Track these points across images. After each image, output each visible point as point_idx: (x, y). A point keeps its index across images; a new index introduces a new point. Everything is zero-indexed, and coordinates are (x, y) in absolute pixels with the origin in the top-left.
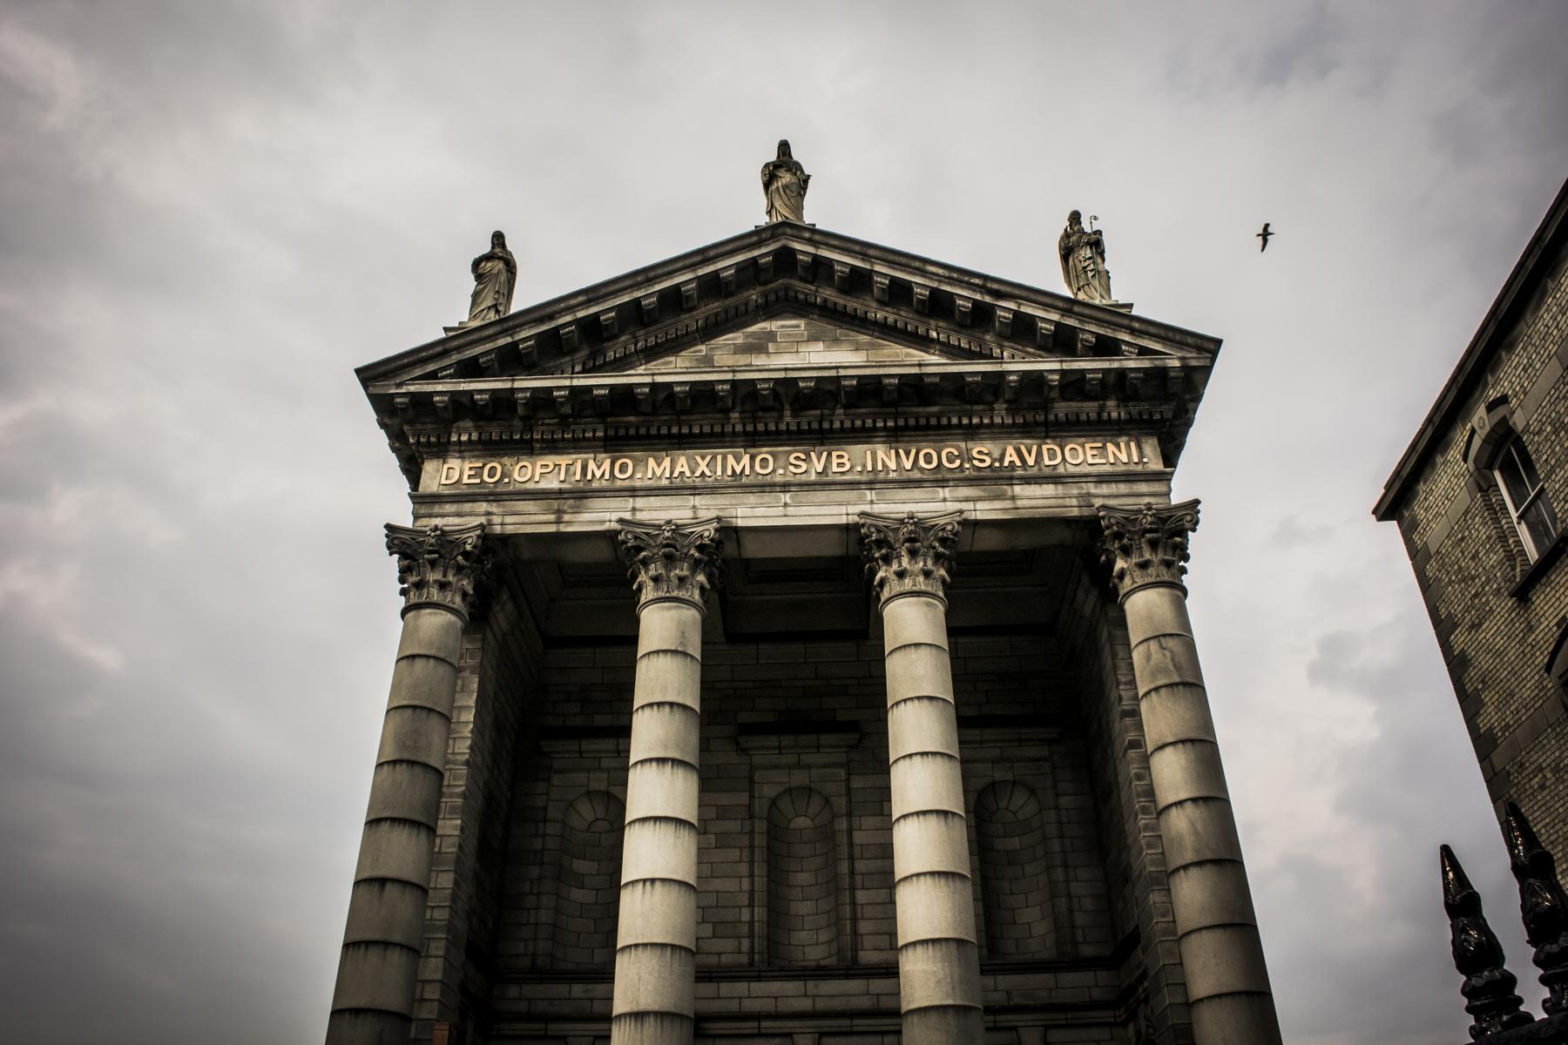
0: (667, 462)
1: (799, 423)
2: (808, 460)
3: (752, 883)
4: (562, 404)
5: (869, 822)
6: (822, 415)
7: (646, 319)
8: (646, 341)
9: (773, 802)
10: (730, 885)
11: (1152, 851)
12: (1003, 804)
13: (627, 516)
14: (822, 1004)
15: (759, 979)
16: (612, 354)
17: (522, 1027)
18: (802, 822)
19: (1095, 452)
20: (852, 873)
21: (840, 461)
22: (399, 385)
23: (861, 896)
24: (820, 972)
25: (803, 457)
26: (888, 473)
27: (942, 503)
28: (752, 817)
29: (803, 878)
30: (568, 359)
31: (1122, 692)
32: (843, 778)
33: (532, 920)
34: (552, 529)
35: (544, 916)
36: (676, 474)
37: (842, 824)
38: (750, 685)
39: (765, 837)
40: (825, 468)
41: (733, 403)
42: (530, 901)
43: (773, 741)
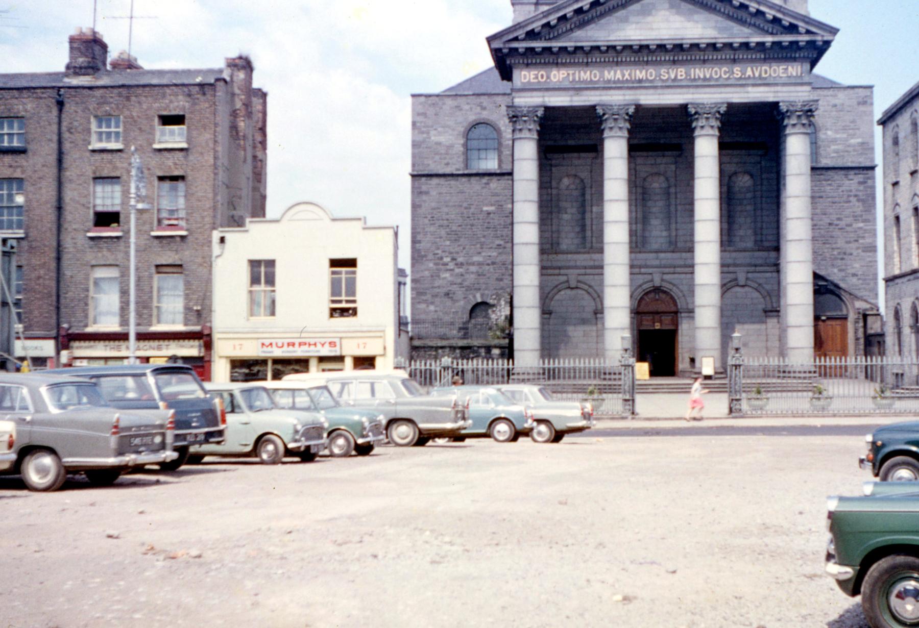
0: (612, 73)
2: (668, 73)
25: (666, 71)
28: (636, 187)
40: (676, 76)
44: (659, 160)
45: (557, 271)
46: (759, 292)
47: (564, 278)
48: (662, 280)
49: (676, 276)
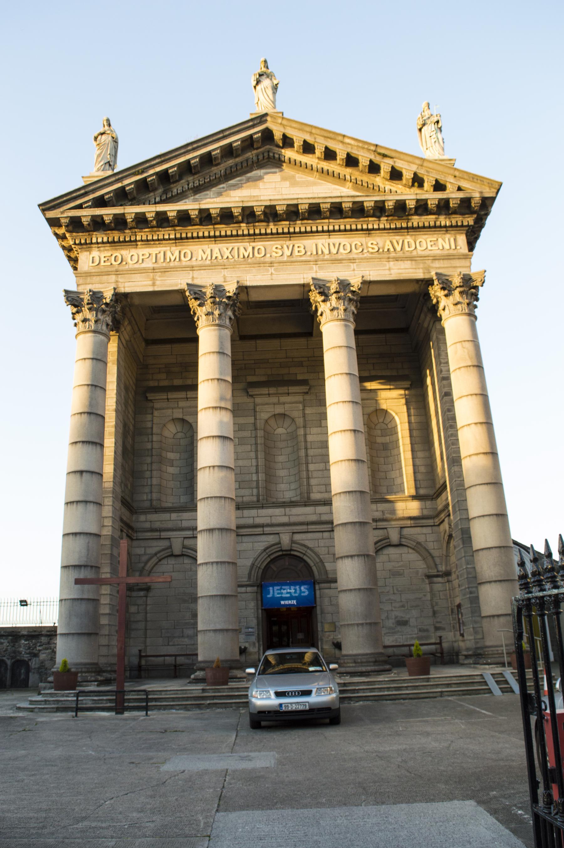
1: (277, 229)
3: (257, 462)
4: (151, 221)
5: (314, 430)
6: (290, 224)
7: (193, 171)
8: (194, 183)
9: (266, 421)
10: (246, 463)
11: (455, 447)
12: (381, 420)
13: (190, 282)
14: (294, 519)
15: (262, 507)
16: (176, 190)
17: (148, 535)
18: (280, 431)
19: (432, 243)
20: (307, 456)
21: (299, 249)
22: (62, 213)
23: (311, 467)
24: (292, 504)
26: (324, 256)
27: (353, 272)
28: (256, 429)
29: (281, 459)
30: (152, 194)
31: (442, 368)
32: (301, 409)
33: (149, 483)
34: (150, 289)
35: (155, 481)
36: (214, 258)
37: (301, 432)
38: (253, 362)
39: (263, 439)
41: (243, 219)
42: (148, 474)
43: (265, 391)
44: (283, 399)
45: (156, 534)
46: (417, 552)
47: (165, 543)
48: (293, 542)
49: (310, 536)
